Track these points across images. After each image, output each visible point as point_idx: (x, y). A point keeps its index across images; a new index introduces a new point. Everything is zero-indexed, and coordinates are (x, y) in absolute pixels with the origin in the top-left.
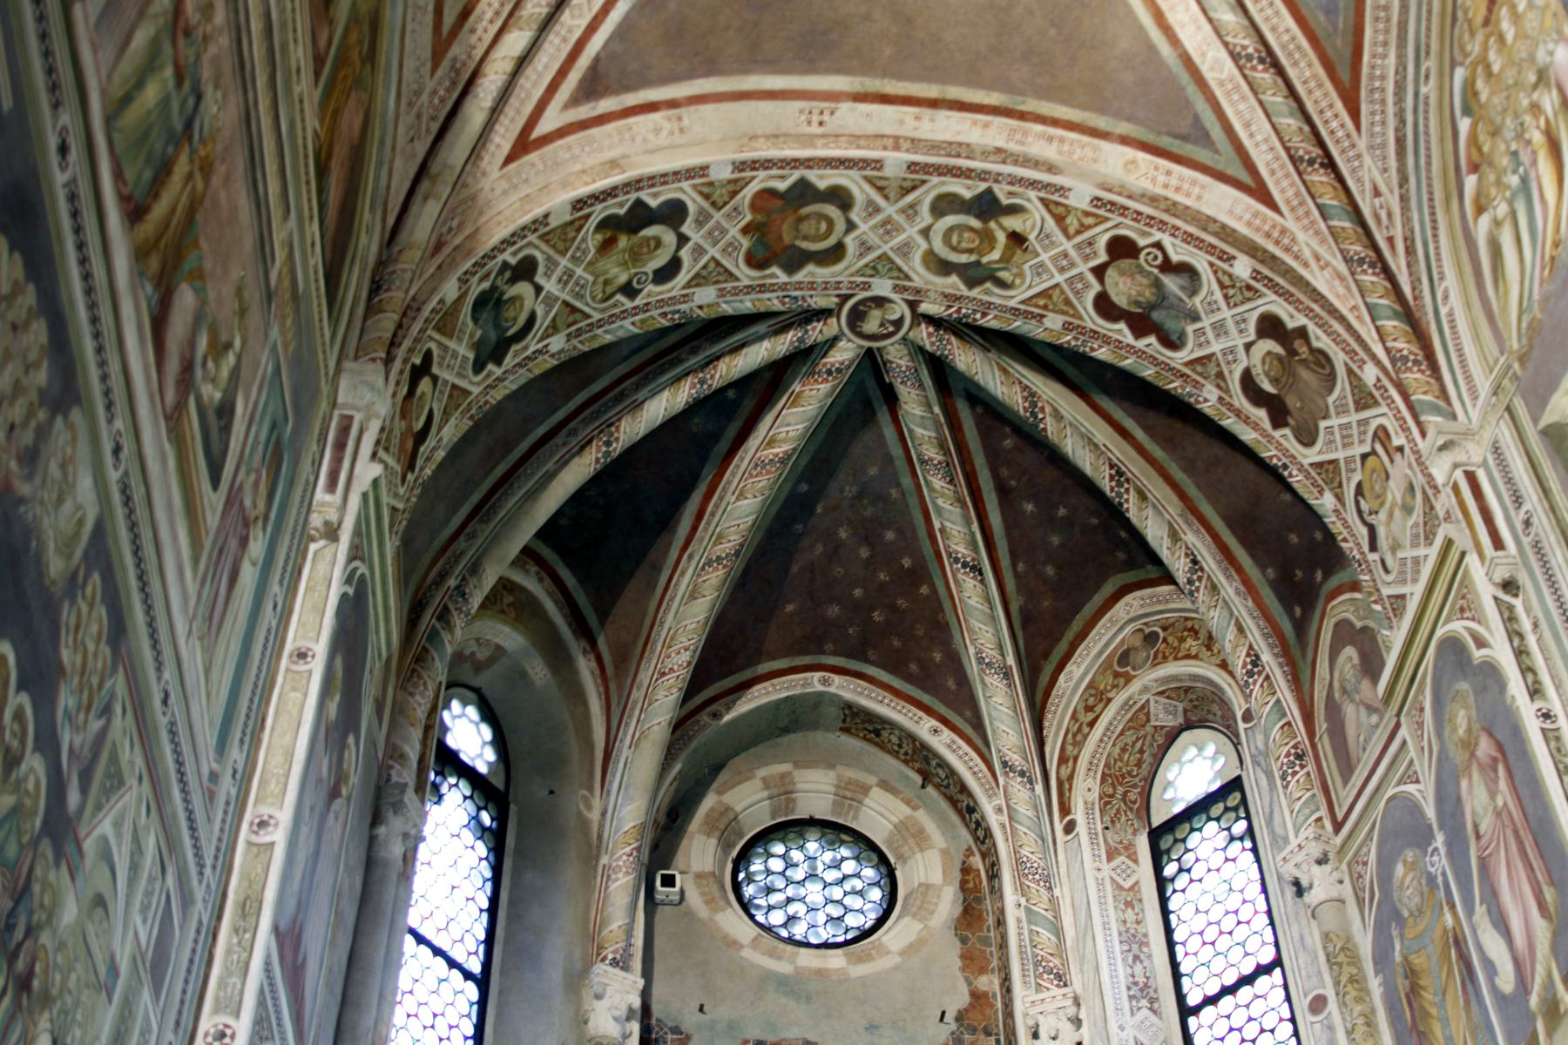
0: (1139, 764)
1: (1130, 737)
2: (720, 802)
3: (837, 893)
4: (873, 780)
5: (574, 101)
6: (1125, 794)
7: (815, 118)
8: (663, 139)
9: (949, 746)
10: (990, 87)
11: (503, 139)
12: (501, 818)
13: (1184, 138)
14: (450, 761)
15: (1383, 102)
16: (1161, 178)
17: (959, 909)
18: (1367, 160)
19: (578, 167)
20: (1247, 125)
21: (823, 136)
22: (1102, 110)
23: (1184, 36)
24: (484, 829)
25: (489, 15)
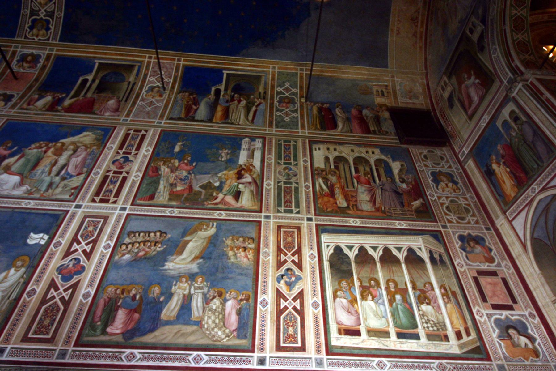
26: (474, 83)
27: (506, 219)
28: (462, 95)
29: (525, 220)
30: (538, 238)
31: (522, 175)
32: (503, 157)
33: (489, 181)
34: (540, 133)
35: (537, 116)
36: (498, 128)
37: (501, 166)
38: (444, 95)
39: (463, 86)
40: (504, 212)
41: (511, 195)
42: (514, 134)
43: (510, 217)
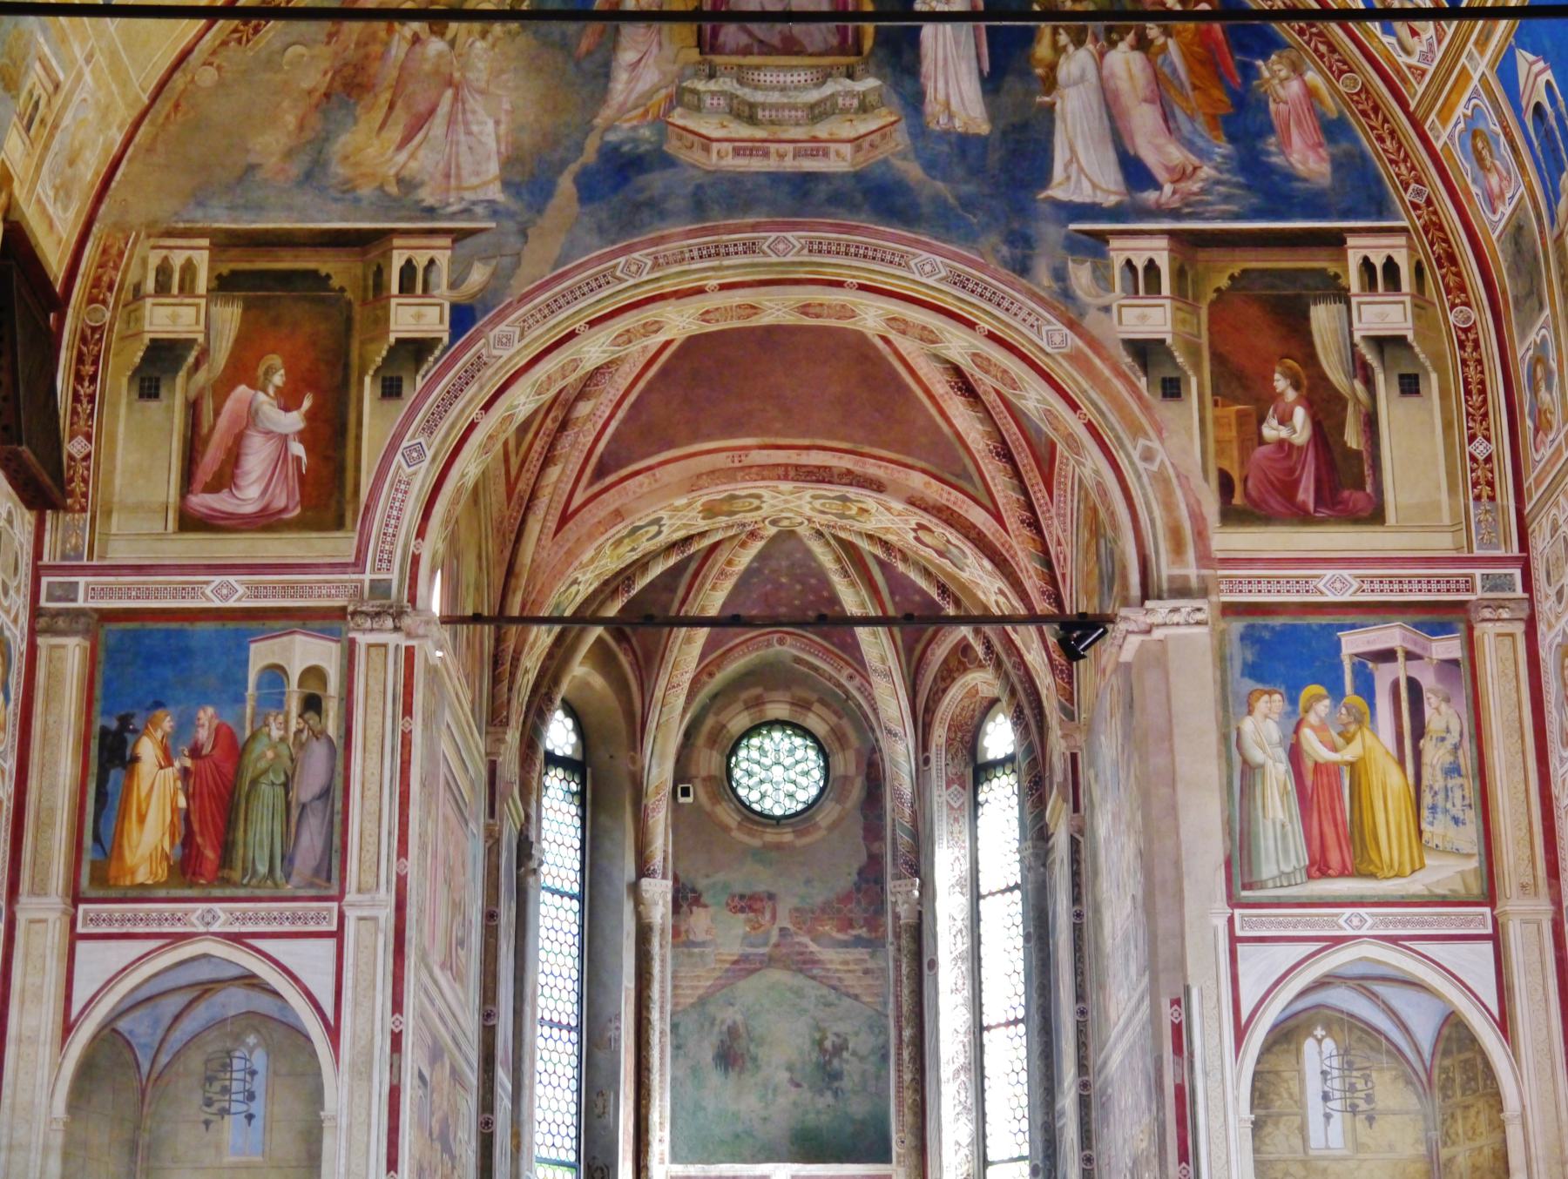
0: (972, 717)
1: (966, 702)
2: (717, 722)
3: (792, 775)
4: (814, 697)
5: (591, 483)
6: (962, 738)
7: (736, 459)
8: (645, 489)
9: (859, 689)
10: (843, 439)
11: (552, 525)
12: (583, 783)
13: (957, 476)
14: (552, 760)
15: (1065, 491)
16: (945, 495)
17: (864, 794)
18: (1056, 521)
19: (596, 520)
20: (993, 478)
21: (742, 468)
22: (908, 454)
23: (955, 422)
24: (573, 794)
25: (536, 456)
26: (284, 438)
27: (67, 919)
28: (217, 413)
29: (124, 969)
30: (126, 1034)
31: (210, 854)
32: (195, 752)
33: (94, 768)
34: (338, 806)
35: (364, 760)
36: (246, 662)
37: (171, 772)
38: (149, 301)
39: (242, 389)
40: (76, 899)
41: (133, 873)
42: (276, 733)
43: (85, 925)
